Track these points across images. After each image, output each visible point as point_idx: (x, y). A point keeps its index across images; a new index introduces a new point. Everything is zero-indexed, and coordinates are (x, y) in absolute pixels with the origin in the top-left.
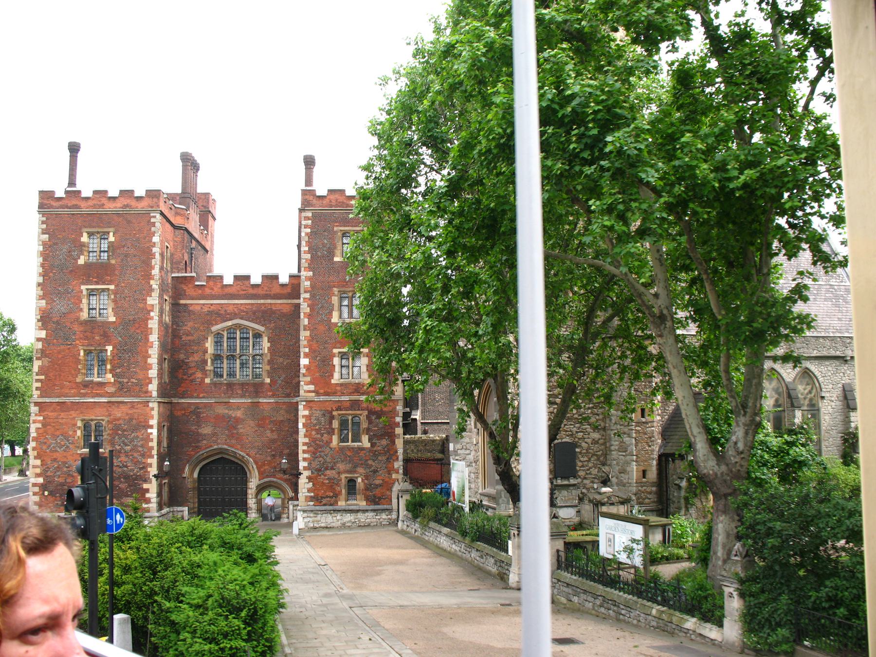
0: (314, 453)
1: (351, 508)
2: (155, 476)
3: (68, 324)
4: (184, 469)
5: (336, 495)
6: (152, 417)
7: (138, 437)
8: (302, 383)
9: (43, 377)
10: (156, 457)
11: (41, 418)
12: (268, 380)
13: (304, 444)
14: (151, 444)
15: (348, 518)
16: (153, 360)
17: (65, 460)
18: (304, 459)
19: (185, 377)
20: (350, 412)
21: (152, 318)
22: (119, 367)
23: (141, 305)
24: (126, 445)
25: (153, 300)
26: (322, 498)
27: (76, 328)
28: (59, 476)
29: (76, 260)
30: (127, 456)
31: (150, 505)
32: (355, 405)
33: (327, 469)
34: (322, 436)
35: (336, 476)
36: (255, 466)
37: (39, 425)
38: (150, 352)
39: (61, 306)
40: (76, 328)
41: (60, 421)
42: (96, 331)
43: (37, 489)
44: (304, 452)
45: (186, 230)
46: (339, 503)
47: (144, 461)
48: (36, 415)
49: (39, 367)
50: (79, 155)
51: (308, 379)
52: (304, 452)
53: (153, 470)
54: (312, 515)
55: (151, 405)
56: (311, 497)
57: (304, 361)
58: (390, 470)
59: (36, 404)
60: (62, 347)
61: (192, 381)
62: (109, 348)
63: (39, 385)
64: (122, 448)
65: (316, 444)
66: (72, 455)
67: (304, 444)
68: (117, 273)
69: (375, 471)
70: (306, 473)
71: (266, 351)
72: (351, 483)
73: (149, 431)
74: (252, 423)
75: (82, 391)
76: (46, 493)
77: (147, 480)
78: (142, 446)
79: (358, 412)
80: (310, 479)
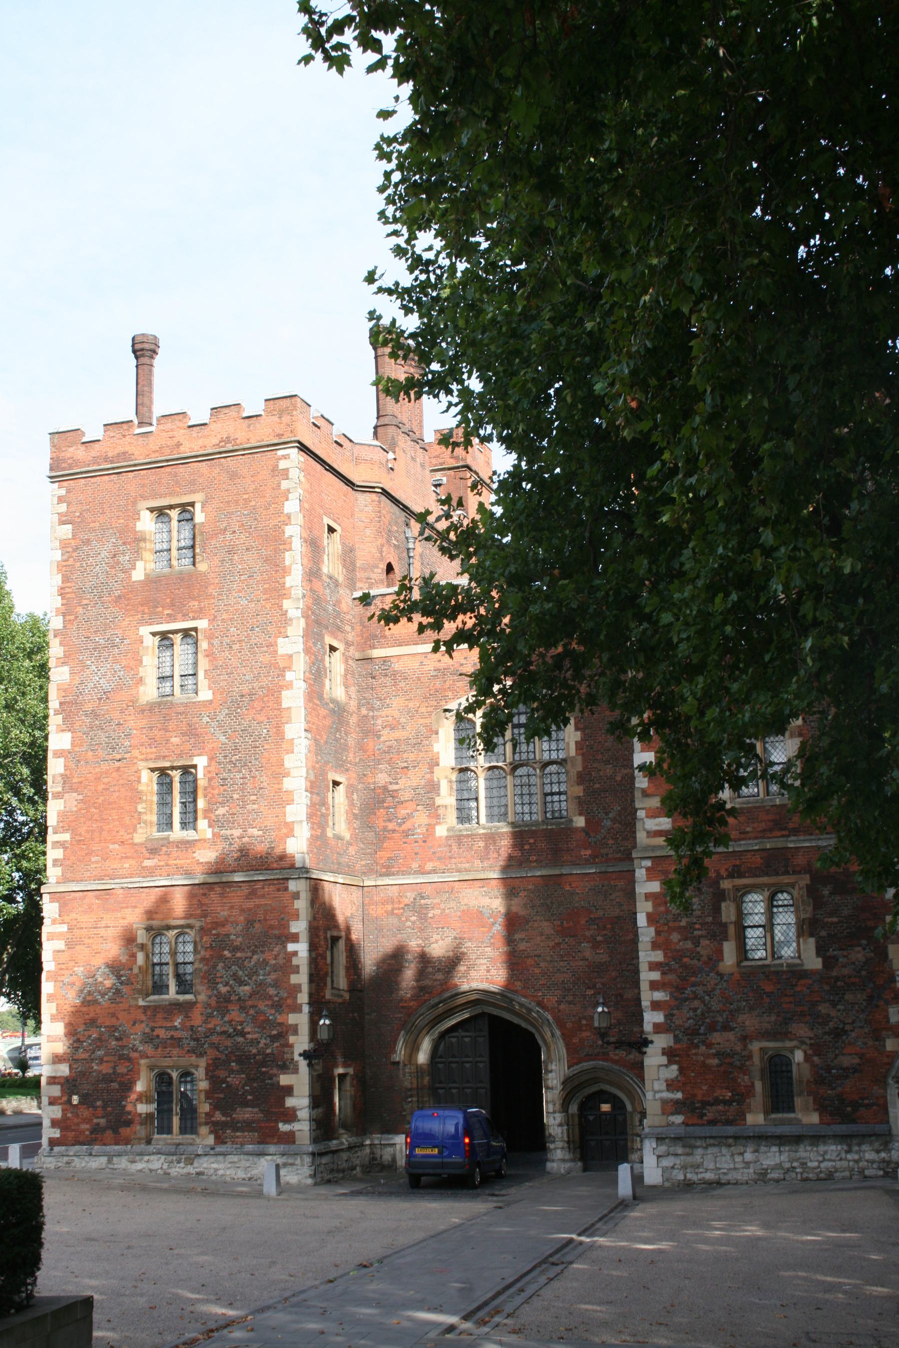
0: (680, 989)
1: (779, 1130)
2: (305, 1055)
3: (116, 715)
4: (395, 1042)
5: (741, 1097)
6: (296, 916)
7: (265, 962)
8: (641, 814)
9: (66, 837)
10: (306, 1009)
11: (64, 928)
12: (580, 822)
13: (653, 966)
14: (294, 979)
15: (773, 1157)
16: (296, 782)
17: (114, 1021)
18: (656, 1006)
19: (391, 826)
20: (765, 880)
21: (289, 686)
22: (223, 804)
23: (265, 659)
24: (241, 983)
25: (292, 644)
26: (705, 1104)
28: (101, 1061)
29: (127, 572)
30: (243, 1009)
31: (296, 1126)
33: (712, 1028)
34: (697, 943)
35: (738, 1048)
36: (558, 1033)
37: (60, 945)
38: (287, 764)
39: (100, 676)
40: (133, 722)
41: (102, 932)
42: (171, 725)
43: (56, 1091)
44: (654, 986)
45: (385, 493)
46: (750, 1119)
47: (280, 1019)
48: (54, 922)
49: (59, 814)
50: (157, 361)
51: (655, 802)
52: (654, 986)
53: (301, 1043)
54: (680, 1150)
55: (292, 886)
56: (676, 1102)
60: (104, 767)
61: (406, 834)
62: (201, 762)
64: (232, 992)
65: (685, 966)
66: (128, 1010)
67: (653, 966)
68: (211, 590)
69: (838, 1033)
70: (661, 1041)
71: (573, 752)
72: (777, 1070)
73: (291, 947)
74: (547, 927)
75: (147, 863)
76: (75, 1099)
77: (288, 1066)
78: (276, 984)
79: (786, 879)
80: (670, 1054)
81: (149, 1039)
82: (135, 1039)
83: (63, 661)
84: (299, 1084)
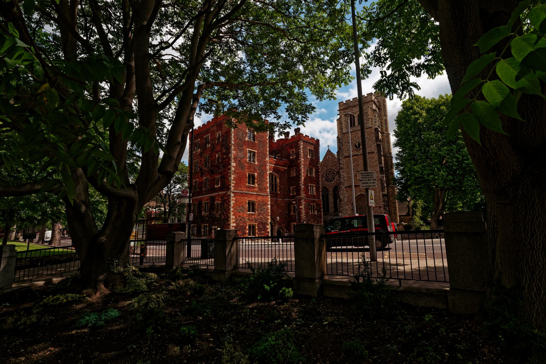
27: (246, 164)
32: (314, 202)
39: (240, 155)
40: (246, 164)
57: (303, 187)
58: (321, 222)
59: (233, 193)
62: (256, 174)
63: (233, 185)
77: (268, 225)
81: (249, 219)
82: (246, 220)
83: (235, 150)
84: (269, 227)
